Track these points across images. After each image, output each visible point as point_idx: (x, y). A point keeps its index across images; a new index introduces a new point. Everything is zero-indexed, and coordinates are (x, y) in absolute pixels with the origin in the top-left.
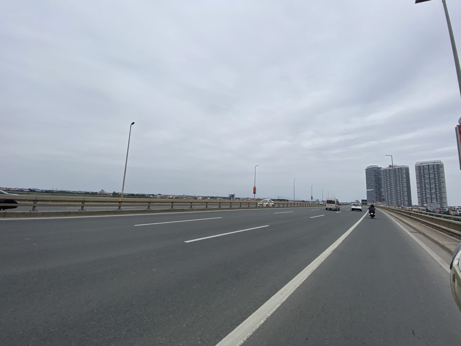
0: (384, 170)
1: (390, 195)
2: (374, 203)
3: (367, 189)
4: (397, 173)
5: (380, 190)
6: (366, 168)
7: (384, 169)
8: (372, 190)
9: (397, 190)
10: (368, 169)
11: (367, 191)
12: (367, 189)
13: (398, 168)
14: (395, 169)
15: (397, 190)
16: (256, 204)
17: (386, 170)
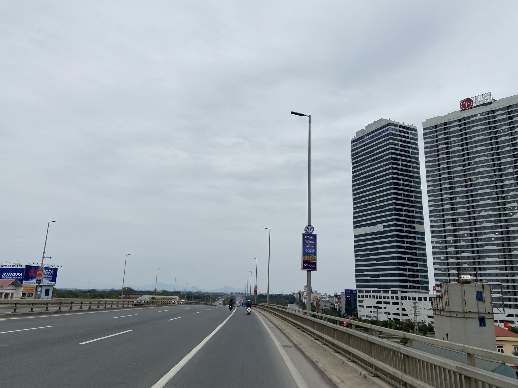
0: (436, 127)
1: (467, 246)
2: (390, 295)
3: (357, 225)
4: (504, 130)
5: (414, 227)
6: (354, 136)
7: (438, 123)
8: (380, 228)
9: (506, 221)
10: (363, 137)
11: (355, 236)
12: (355, 227)
13: (509, 107)
14: (493, 112)
15: (506, 221)
16: (46, 306)
17: (445, 124)
